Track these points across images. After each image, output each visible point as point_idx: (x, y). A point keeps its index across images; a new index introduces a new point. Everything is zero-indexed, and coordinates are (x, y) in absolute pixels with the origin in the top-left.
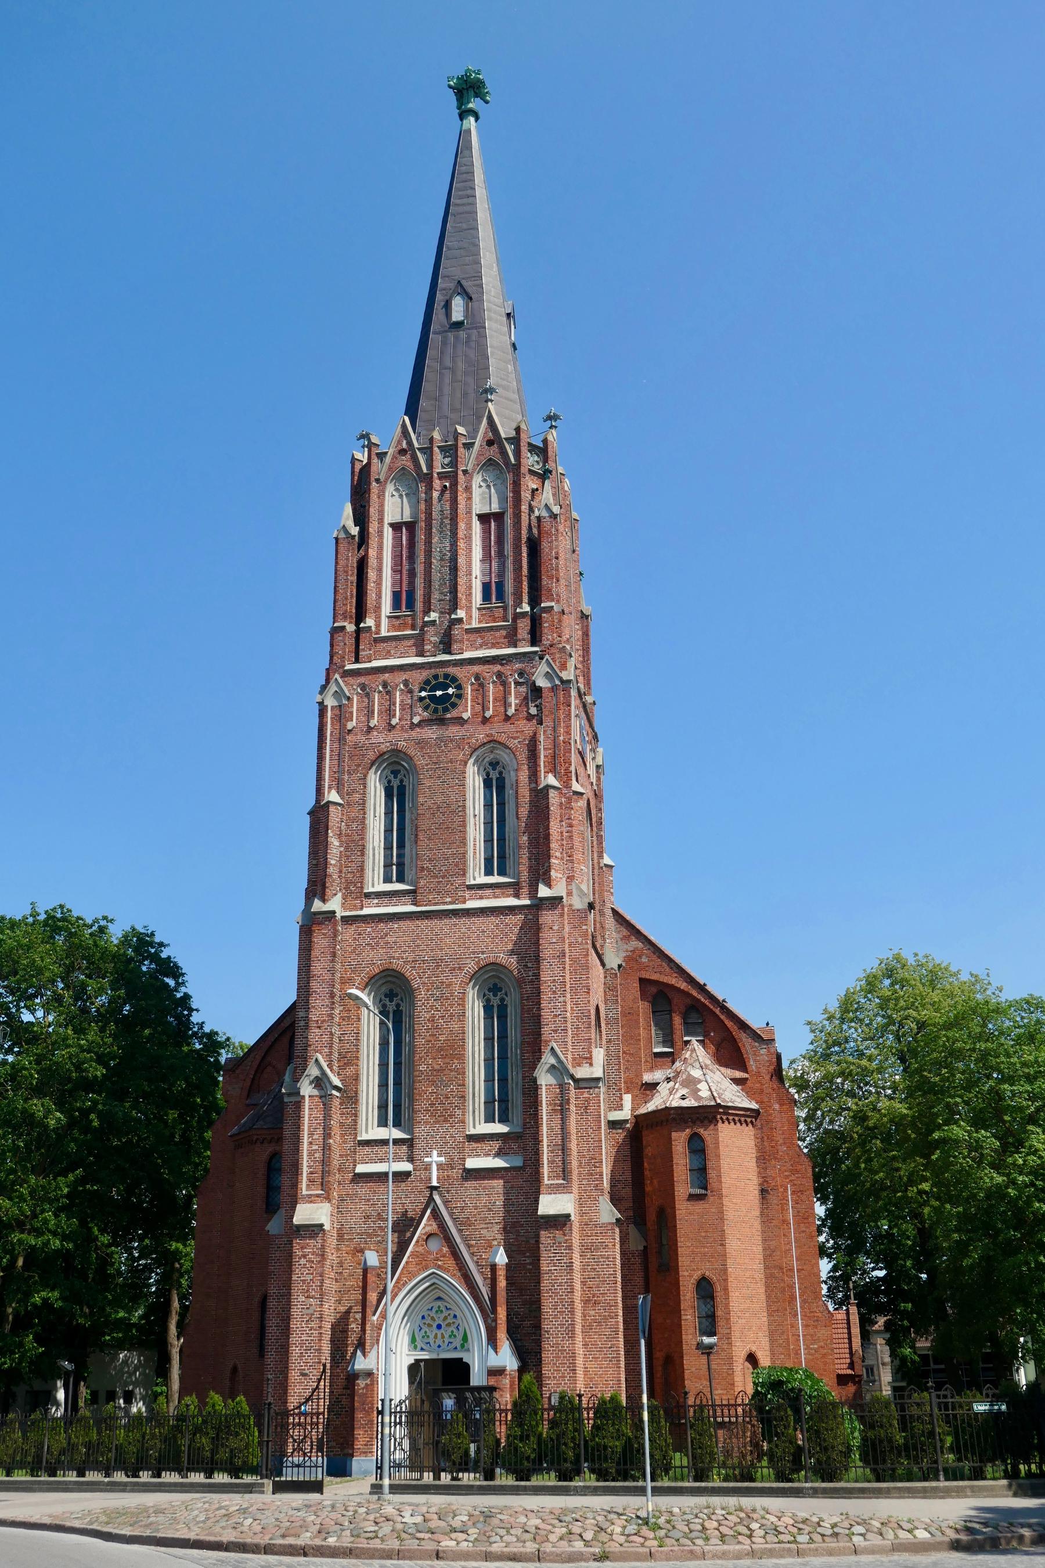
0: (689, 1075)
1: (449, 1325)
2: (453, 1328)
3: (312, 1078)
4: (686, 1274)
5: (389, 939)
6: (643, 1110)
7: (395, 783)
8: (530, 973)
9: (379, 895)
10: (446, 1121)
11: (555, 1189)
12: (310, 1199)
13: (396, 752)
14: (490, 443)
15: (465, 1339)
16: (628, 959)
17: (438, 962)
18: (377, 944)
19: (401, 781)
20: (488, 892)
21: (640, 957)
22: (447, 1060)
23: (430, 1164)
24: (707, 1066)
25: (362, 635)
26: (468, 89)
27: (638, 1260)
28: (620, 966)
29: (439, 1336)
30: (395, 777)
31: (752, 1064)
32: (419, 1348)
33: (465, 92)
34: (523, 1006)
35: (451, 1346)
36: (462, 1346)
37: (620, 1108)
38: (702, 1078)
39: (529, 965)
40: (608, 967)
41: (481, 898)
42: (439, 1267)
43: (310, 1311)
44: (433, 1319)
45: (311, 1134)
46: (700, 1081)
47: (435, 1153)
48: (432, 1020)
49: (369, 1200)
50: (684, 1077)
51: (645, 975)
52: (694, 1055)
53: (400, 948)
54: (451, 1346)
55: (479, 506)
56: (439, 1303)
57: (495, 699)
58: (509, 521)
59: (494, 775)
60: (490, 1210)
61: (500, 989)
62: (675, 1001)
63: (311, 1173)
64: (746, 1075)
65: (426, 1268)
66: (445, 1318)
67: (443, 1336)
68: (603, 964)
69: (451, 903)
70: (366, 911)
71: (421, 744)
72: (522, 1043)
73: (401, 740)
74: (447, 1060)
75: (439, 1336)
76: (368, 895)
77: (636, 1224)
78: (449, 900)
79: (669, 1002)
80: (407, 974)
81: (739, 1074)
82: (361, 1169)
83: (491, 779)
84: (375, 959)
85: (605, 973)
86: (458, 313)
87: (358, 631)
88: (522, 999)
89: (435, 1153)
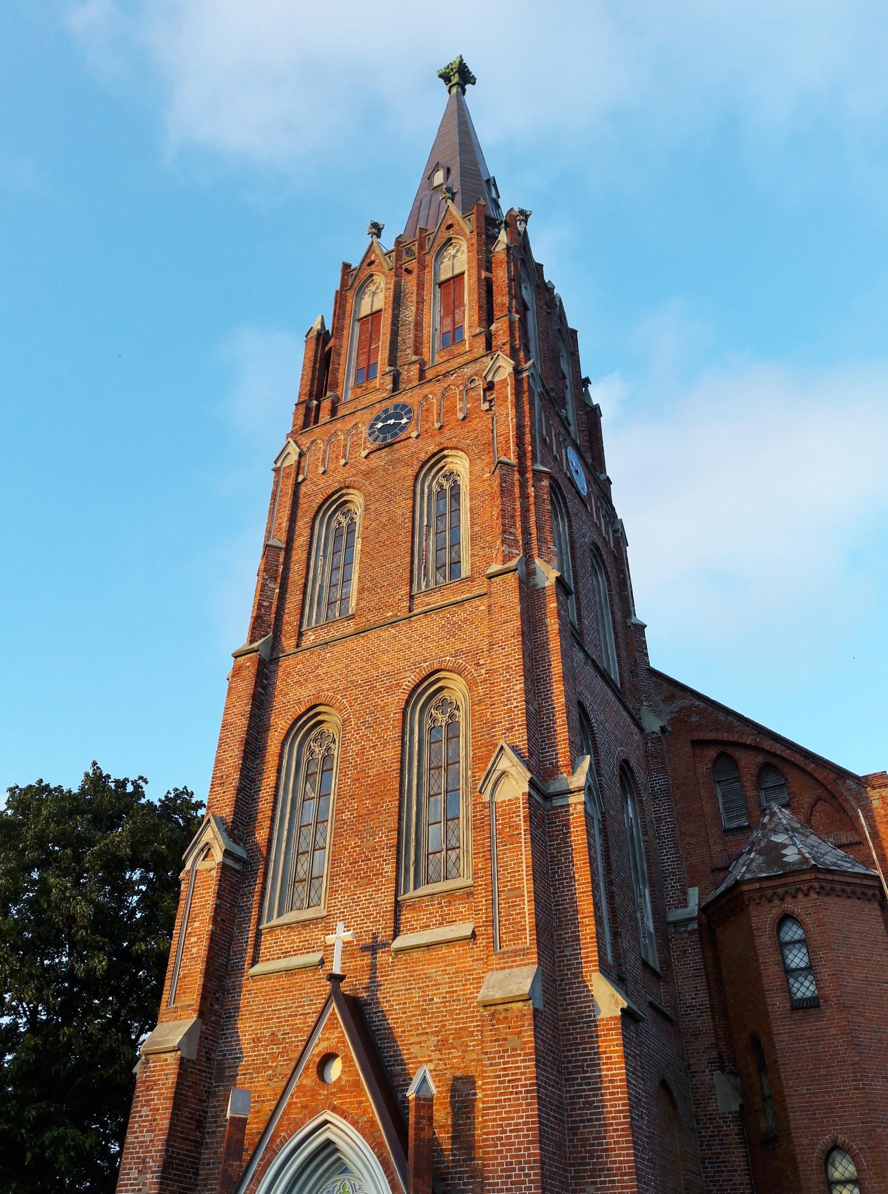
0: (770, 841)
4: (805, 1141)
5: (320, 671)
6: (711, 897)
8: (483, 672)
10: (370, 882)
16: (673, 722)
21: (689, 717)
22: (376, 801)
24: (794, 830)
27: (734, 1128)
28: (663, 729)
34: (473, 712)
37: (684, 903)
38: (788, 842)
40: (648, 731)
42: (334, 1109)
46: (785, 846)
47: (340, 926)
50: (763, 844)
51: (697, 736)
52: (775, 819)
59: (447, 486)
60: (424, 1012)
62: (742, 763)
64: (858, 839)
65: (315, 1112)
68: (642, 730)
74: (376, 801)
77: (722, 1069)
78: (391, 614)
79: (734, 763)
85: (645, 738)
89: (340, 926)
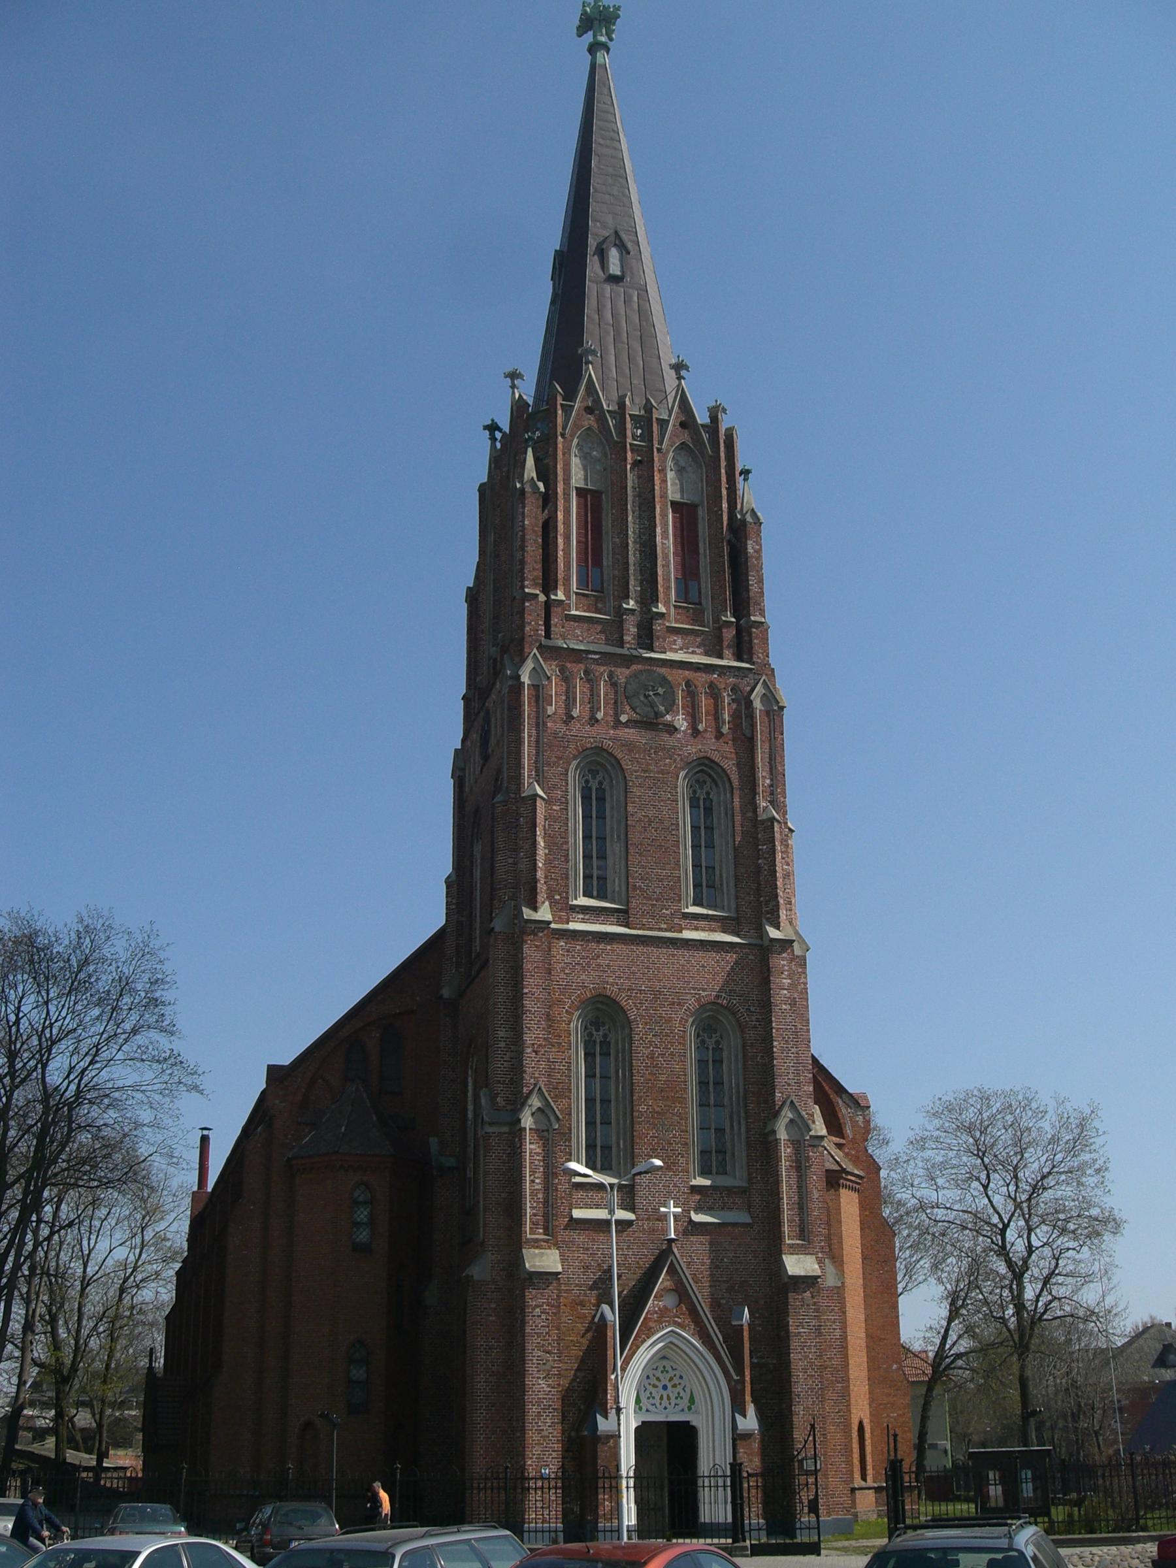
1: (674, 1386)
2: (679, 1389)
3: (534, 1109)
7: (594, 785)
9: (585, 909)
11: (795, 1250)
12: (536, 1244)
13: (600, 750)
14: (683, 425)
15: (692, 1400)
17: (657, 994)
18: (589, 964)
19: (708, 794)
20: (703, 923)
23: (665, 1217)
25: (555, 610)
26: (597, 21)
29: (665, 1397)
30: (594, 778)
31: (848, 1131)
32: (644, 1409)
33: (596, 23)
35: (678, 1408)
36: (690, 1408)
39: (752, 1009)
41: (696, 929)
43: (547, 1367)
44: (658, 1379)
45: (533, 1172)
48: (651, 1056)
49: (587, 1249)
53: (616, 973)
54: (678, 1408)
55: (673, 494)
56: (665, 1362)
57: (707, 713)
58: (702, 513)
61: (716, 1031)
63: (535, 1215)
64: (842, 1141)
66: (671, 1379)
67: (669, 1398)
69: (666, 930)
70: (573, 926)
71: (630, 746)
72: (746, 1091)
73: (604, 735)
75: (665, 1397)
76: (574, 909)
78: (664, 926)
80: (623, 1003)
81: (837, 1140)
82: (577, 1214)
83: (699, 799)
84: (587, 981)
86: (615, 268)
87: (548, 605)
88: (744, 1046)
